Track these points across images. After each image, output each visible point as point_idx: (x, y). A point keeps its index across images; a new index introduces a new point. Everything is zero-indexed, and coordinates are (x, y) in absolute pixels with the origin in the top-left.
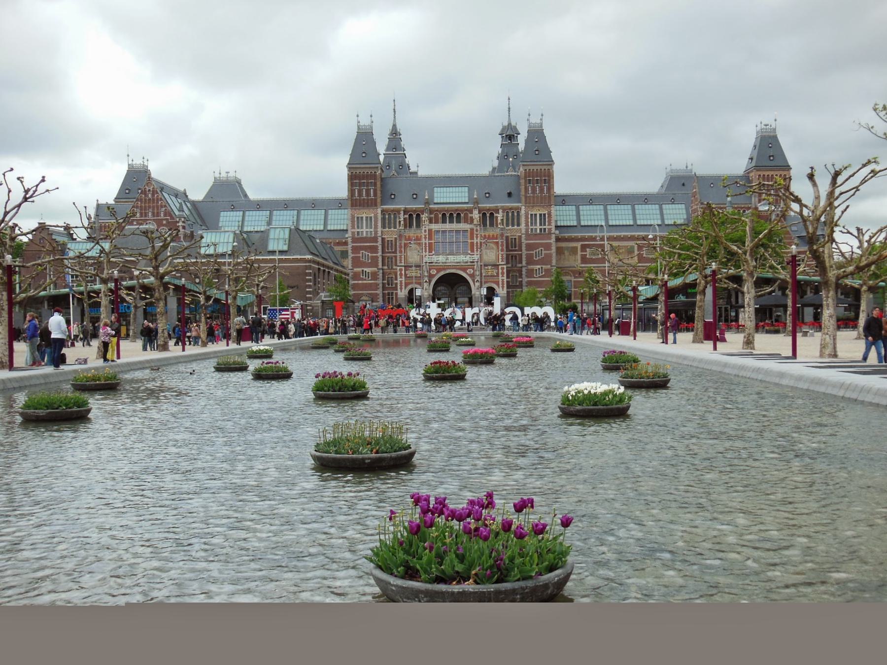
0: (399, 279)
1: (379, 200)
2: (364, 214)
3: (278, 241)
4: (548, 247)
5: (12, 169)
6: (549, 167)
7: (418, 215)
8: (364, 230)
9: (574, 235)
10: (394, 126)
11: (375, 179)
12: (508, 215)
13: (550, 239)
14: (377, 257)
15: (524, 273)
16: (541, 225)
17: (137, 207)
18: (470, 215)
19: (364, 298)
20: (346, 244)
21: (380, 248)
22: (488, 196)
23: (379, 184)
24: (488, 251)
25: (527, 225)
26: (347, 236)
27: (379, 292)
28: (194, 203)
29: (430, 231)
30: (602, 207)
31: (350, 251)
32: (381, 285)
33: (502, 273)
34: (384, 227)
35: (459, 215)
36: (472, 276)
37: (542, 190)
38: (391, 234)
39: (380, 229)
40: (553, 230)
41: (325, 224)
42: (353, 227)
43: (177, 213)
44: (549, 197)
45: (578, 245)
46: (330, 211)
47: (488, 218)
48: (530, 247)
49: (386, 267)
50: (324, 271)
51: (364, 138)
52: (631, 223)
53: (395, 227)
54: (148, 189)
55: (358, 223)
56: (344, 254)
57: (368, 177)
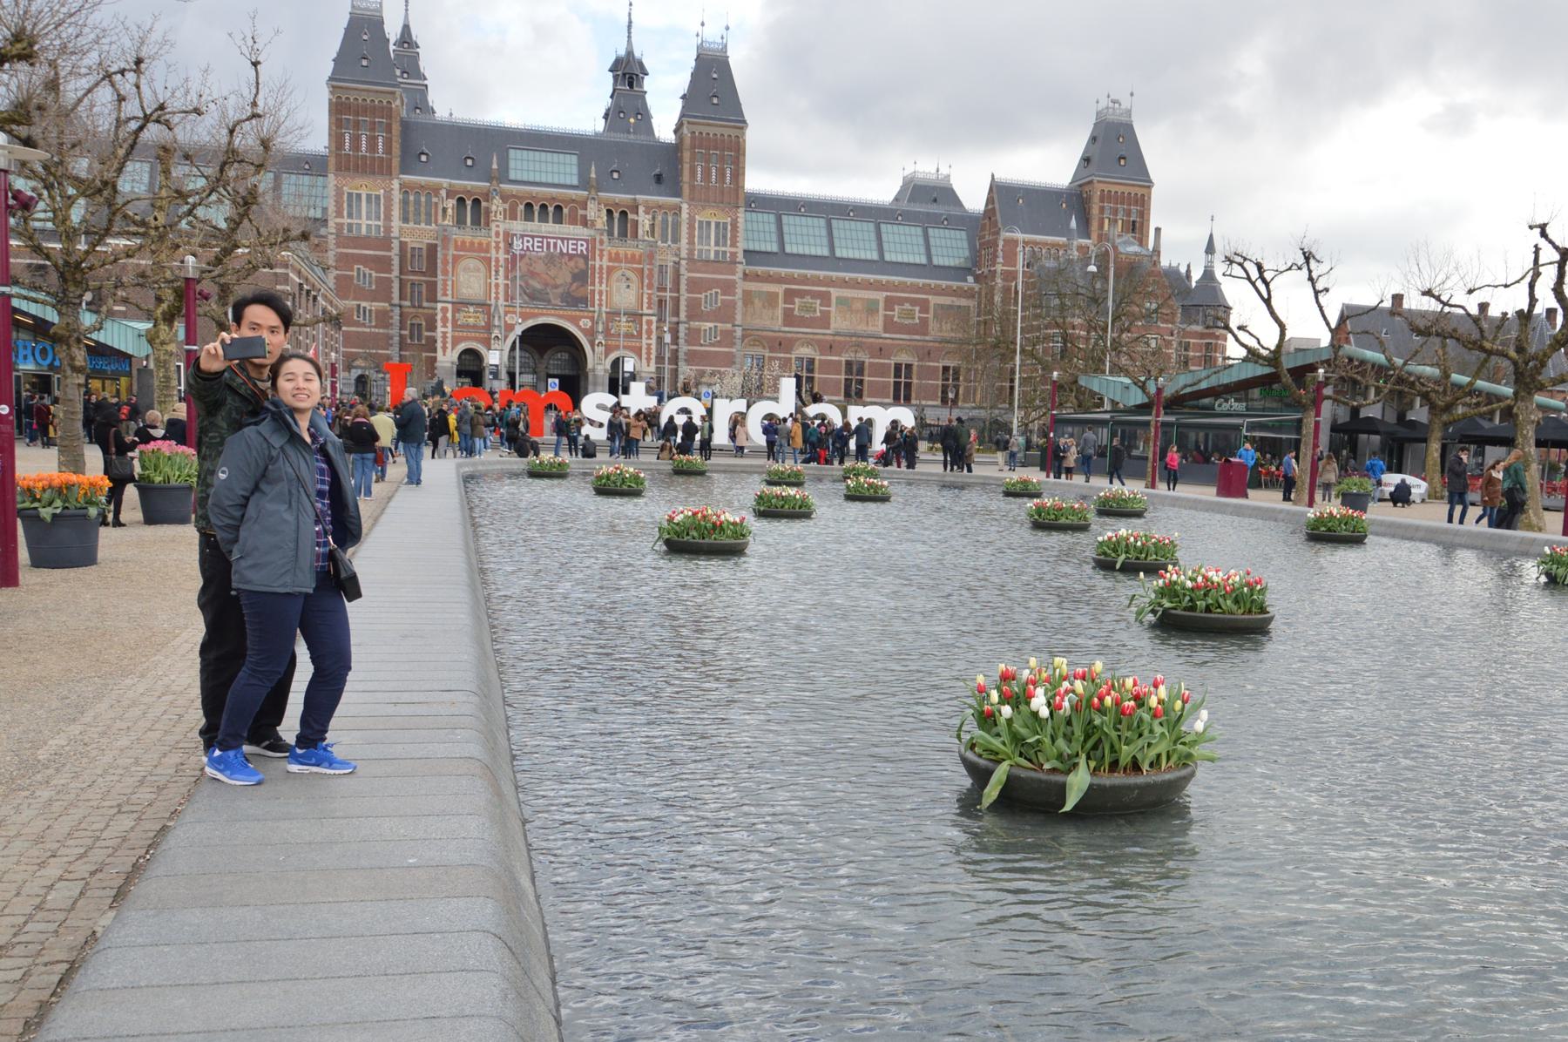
0: (440, 329)
1: (396, 162)
2: (364, 186)
4: (728, 287)
6: (737, 132)
7: (476, 202)
9: (773, 270)
10: (406, 28)
11: (390, 117)
14: (390, 281)
15: (681, 335)
16: (717, 244)
18: (581, 212)
21: (396, 262)
23: (396, 128)
25: (691, 242)
26: (323, 231)
32: (396, 339)
33: (649, 332)
34: (405, 220)
35: (559, 208)
36: (591, 333)
37: (721, 174)
38: (419, 235)
39: (396, 223)
42: (339, 214)
45: (779, 289)
48: (694, 285)
49: (408, 303)
51: (363, 31)
55: (350, 206)
57: (373, 110)
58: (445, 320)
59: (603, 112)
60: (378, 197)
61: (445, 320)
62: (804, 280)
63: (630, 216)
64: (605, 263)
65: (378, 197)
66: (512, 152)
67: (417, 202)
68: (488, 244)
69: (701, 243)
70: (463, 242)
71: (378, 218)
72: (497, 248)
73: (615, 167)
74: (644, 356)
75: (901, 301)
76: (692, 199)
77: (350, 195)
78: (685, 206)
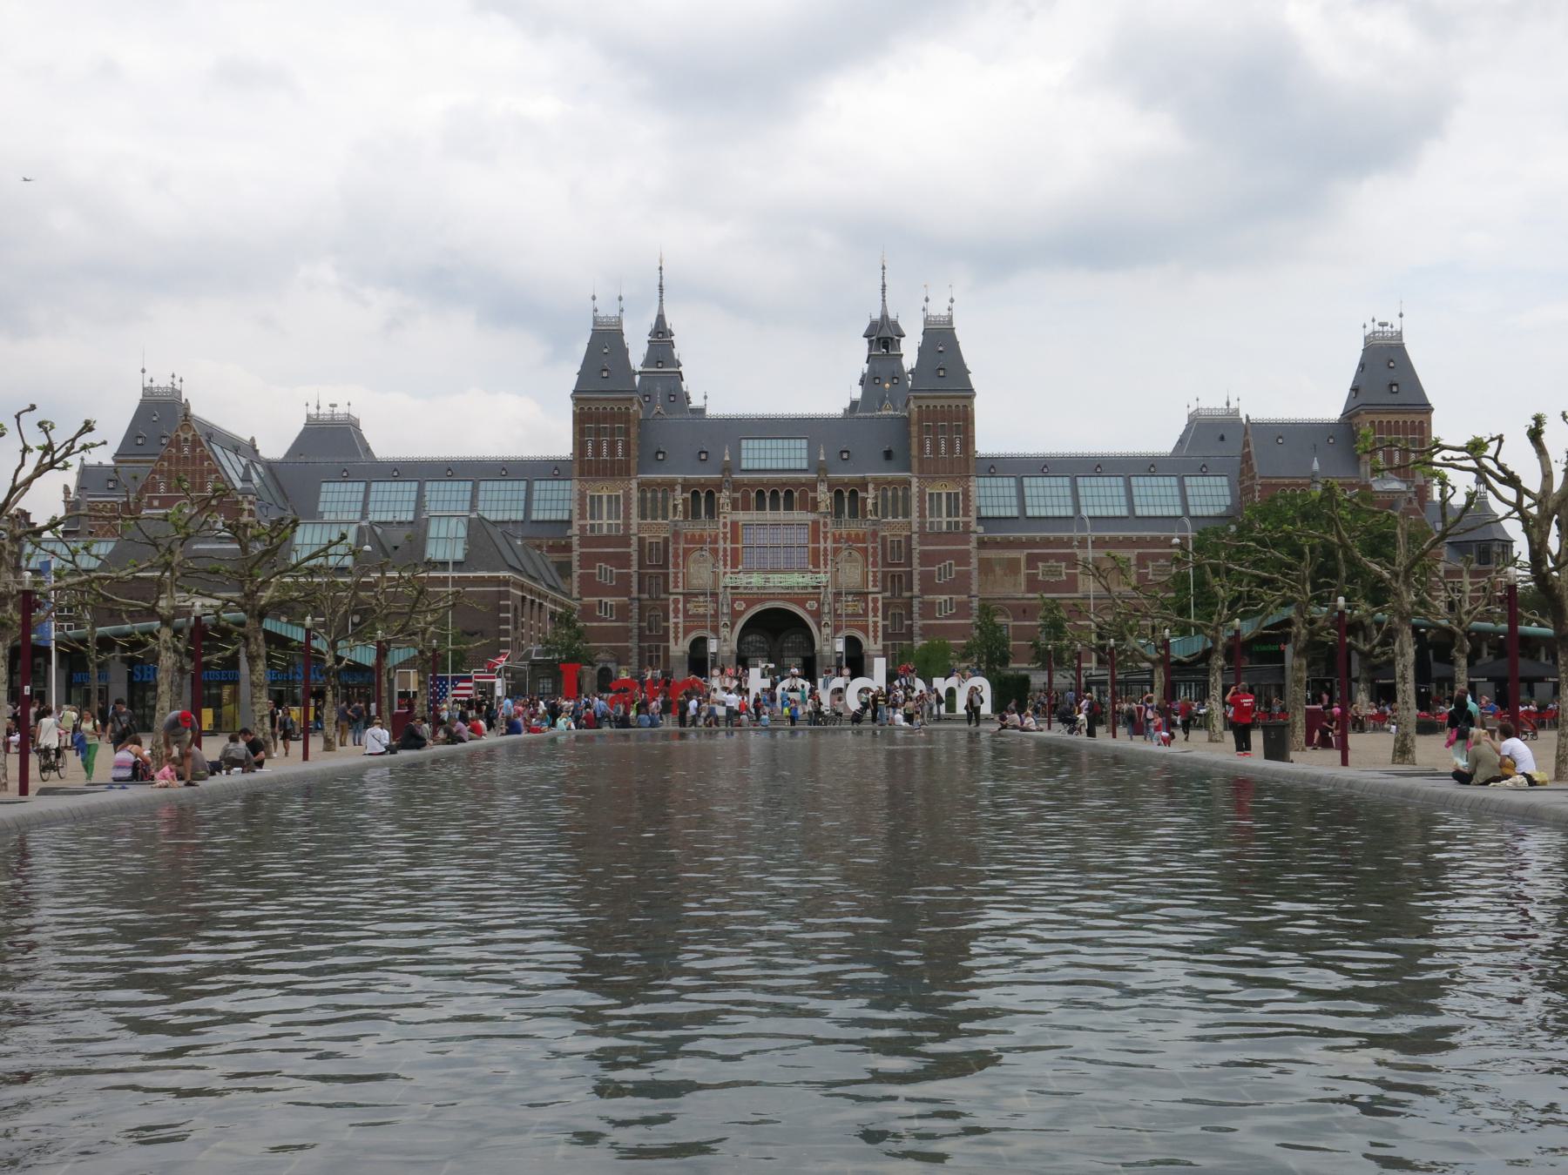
0: (672, 620)
3: (446, 542)
4: (963, 558)
5: (33, 407)
6: (965, 402)
7: (710, 494)
8: (605, 521)
10: (661, 319)
11: (628, 421)
12: (885, 498)
13: (968, 543)
14: (629, 575)
15: (916, 609)
16: (949, 515)
17: (161, 472)
19: (601, 656)
20: (568, 548)
21: (635, 557)
22: (845, 456)
24: (848, 566)
25: (922, 515)
26: (569, 533)
27: (632, 644)
28: (270, 466)
29: (734, 524)
30: (1067, 481)
31: (575, 563)
32: (635, 631)
33: (875, 610)
34: (643, 516)
35: (789, 493)
36: (817, 615)
38: (657, 530)
39: (635, 520)
40: (974, 526)
41: (528, 510)
42: (582, 516)
43: (239, 485)
44: (967, 460)
45: (1021, 555)
46: (537, 485)
47: (848, 499)
48: (927, 558)
49: (646, 596)
50: (533, 602)
51: (606, 343)
52: (1125, 512)
53: (665, 517)
54: (183, 436)
56: (564, 569)
57: (612, 417)
58: (676, 611)
59: (860, 376)
60: (618, 497)
61: (676, 611)
62: (1046, 543)
63: (861, 494)
64: (830, 545)
65: (618, 497)
66: (744, 443)
67: (654, 499)
68: (717, 535)
69: (931, 515)
70: (693, 536)
71: (618, 517)
72: (725, 539)
73: (844, 447)
74: (871, 634)
75: (1155, 557)
76: (921, 472)
77: (592, 497)
78: (915, 481)
